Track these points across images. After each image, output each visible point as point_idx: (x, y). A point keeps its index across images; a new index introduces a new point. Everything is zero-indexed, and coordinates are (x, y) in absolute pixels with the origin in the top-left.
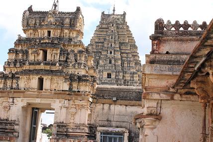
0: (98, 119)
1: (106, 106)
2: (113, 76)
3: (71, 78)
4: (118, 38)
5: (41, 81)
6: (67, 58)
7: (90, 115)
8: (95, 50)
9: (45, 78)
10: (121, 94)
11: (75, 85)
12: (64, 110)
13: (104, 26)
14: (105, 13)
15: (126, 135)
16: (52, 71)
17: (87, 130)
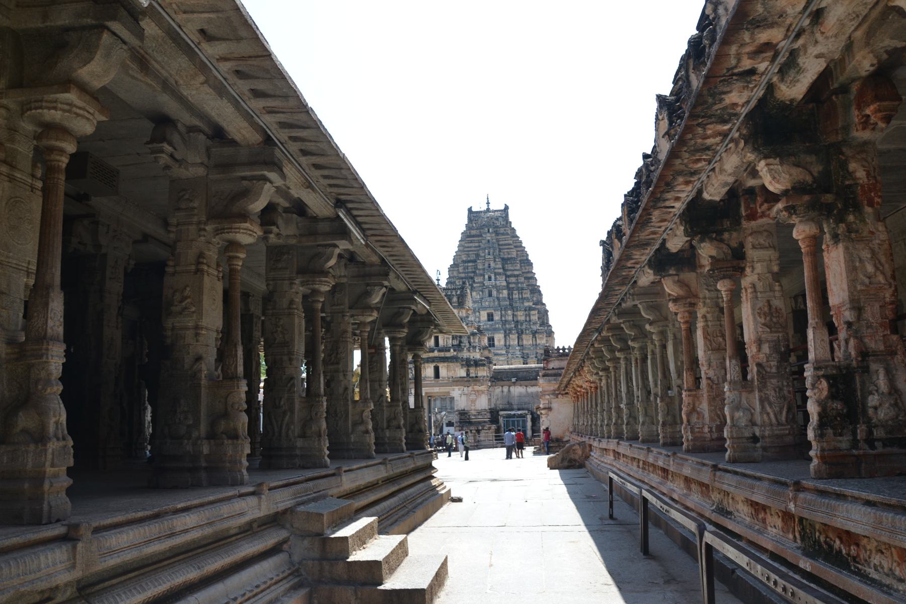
0: (498, 402)
1: (506, 389)
2: (497, 317)
3: (468, 363)
4: (500, 250)
5: (437, 369)
6: (460, 342)
7: (489, 400)
8: (463, 275)
9: (441, 365)
10: (520, 375)
11: (472, 371)
12: (464, 398)
13: (474, 232)
14: (474, 210)
15: (529, 417)
16: (447, 358)
17: (489, 415)
